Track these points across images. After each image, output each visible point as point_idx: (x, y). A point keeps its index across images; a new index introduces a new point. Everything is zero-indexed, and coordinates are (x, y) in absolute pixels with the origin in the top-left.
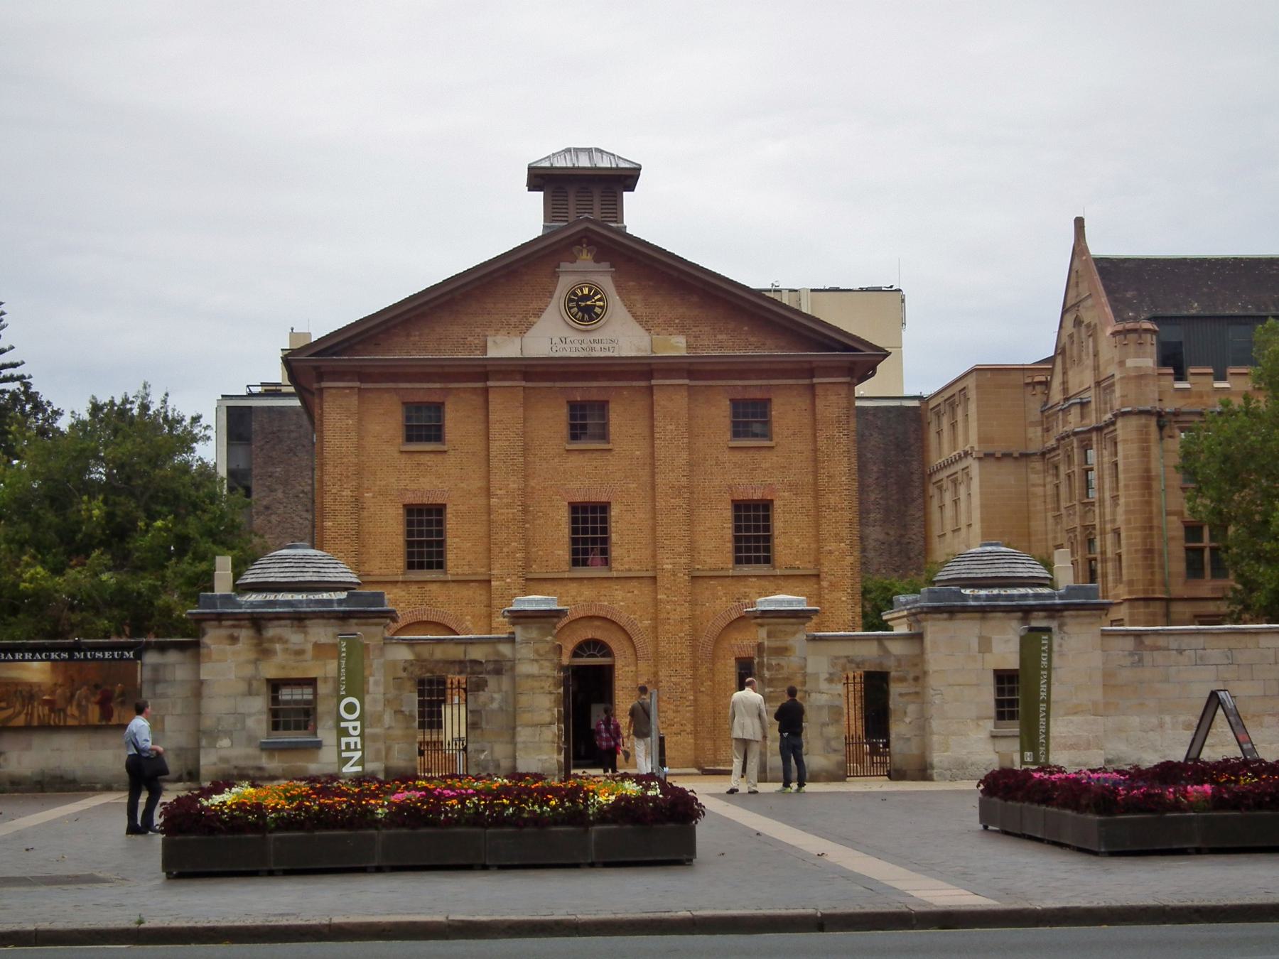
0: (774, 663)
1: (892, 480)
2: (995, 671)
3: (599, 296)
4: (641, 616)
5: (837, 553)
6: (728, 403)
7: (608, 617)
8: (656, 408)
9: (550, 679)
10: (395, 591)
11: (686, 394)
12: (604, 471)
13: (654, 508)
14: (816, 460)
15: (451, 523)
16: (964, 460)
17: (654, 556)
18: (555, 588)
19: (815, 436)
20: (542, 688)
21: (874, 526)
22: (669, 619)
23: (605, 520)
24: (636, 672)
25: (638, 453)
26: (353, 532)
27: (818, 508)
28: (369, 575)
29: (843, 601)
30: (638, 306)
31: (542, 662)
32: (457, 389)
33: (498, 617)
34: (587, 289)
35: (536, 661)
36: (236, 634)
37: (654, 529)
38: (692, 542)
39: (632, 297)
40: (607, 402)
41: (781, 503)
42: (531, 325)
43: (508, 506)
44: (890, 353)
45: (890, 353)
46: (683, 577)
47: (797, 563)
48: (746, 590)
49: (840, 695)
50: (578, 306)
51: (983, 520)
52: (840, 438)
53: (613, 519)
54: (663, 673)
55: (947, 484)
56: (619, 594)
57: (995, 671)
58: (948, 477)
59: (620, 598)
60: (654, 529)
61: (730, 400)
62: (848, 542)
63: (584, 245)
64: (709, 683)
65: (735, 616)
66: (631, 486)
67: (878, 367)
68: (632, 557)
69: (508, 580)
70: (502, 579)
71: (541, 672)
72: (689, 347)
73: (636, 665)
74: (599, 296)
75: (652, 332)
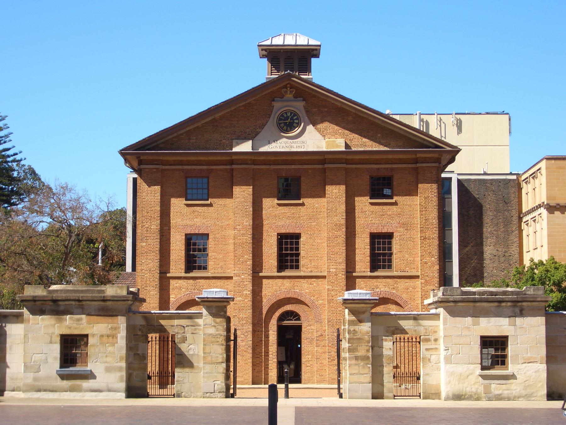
0: (352, 329)
1: (501, 220)
2: (482, 337)
3: (296, 117)
4: (317, 298)
6: (369, 177)
9: (222, 337)
11: (344, 172)
16: (539, 209)
20: (218, 342)
21: (490, 246)
22: (333, 300)
23: (297, 243)
31: (218, 327)
34: (289, 113)
35: (215, 326)
36: (44, 309)
40: (300, 177)
41: (399, 234)
42: (258, 133)
44: (461, 150)
48: (377, 284)
49: (390, 349)
50: (285, 124)
51: (549, 244)
55: (531, 222)
57: (482, 337)
58: (531, 219)
61: (370, 176)
62: (436, 257)
66: (313, 224)
67: (457, 157)
68: (313, 264)
70: (239, 276)
71: (217, 333)
72: (347, 146)
74: (296, 117)
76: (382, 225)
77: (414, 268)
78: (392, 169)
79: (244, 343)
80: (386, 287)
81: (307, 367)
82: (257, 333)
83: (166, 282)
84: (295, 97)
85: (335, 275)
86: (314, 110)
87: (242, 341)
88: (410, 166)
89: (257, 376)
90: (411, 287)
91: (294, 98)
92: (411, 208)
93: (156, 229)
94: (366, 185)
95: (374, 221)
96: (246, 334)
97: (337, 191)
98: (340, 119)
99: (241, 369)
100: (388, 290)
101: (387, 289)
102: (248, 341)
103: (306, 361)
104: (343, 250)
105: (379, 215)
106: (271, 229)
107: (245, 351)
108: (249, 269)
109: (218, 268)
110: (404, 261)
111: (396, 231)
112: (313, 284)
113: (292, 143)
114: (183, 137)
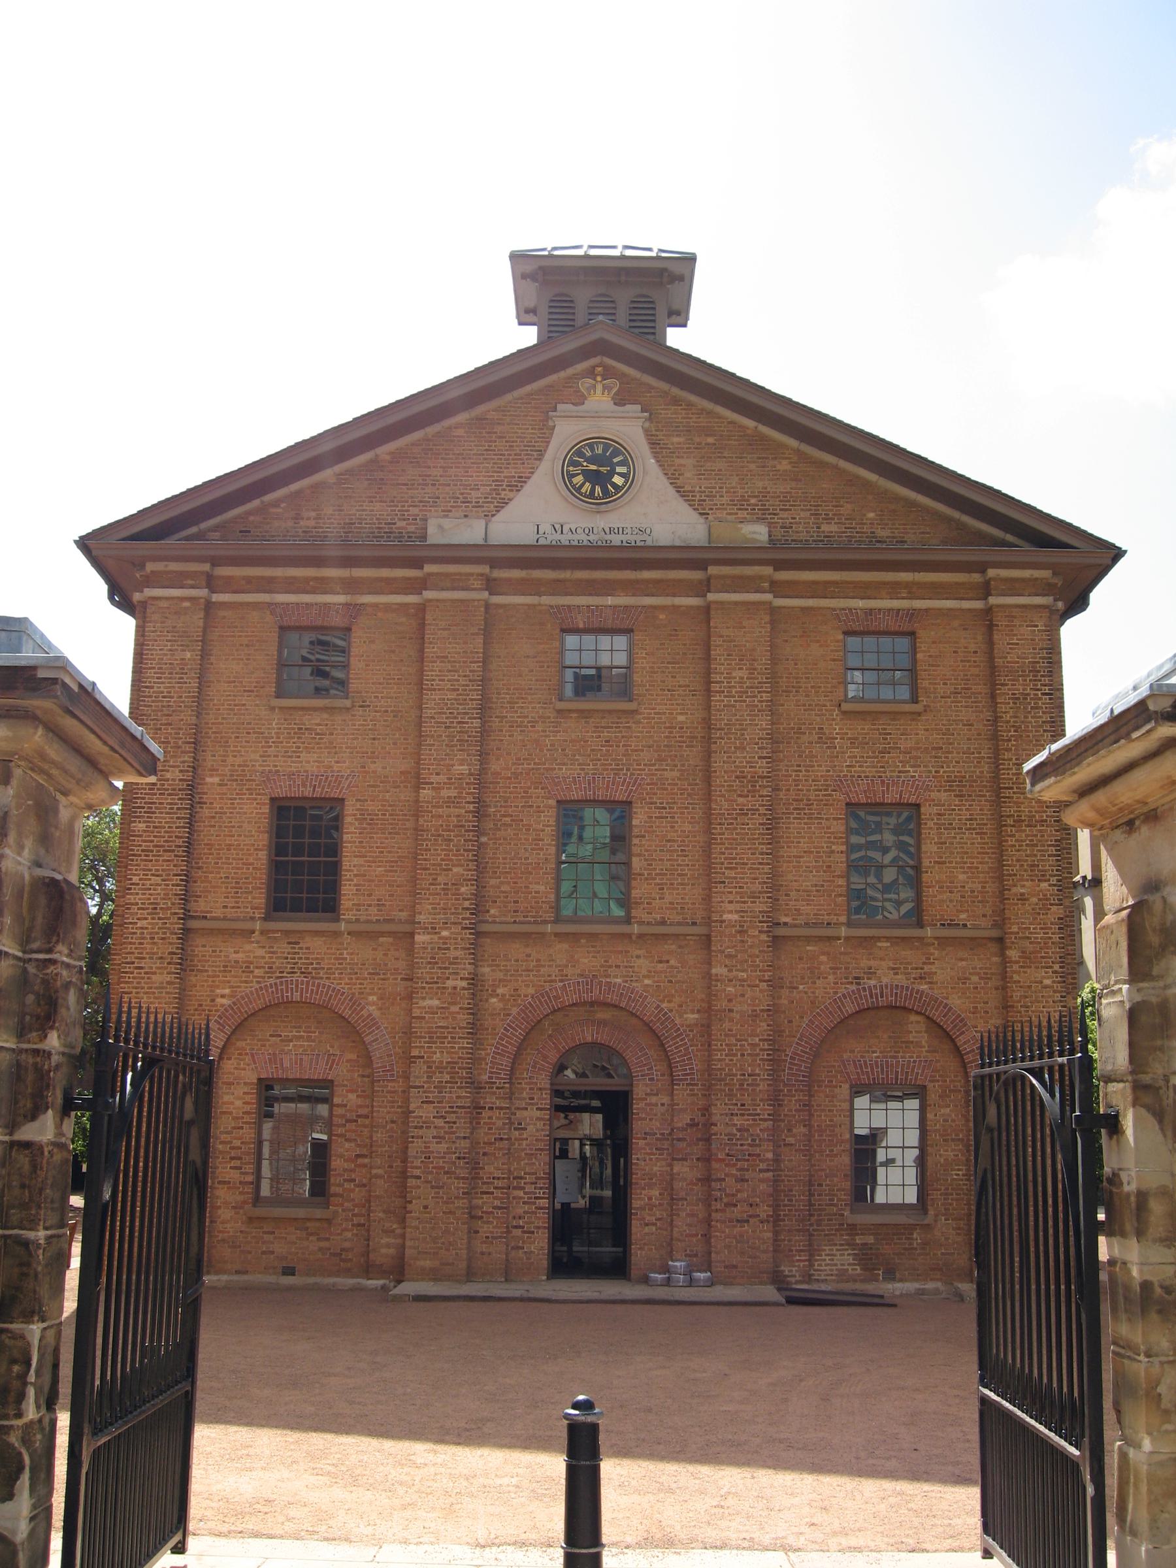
4: (681, 1006)
5: (1034, 900)
7: (623, 1005)
8: (715, 641)
10: (248, 947)
11: (767, 618)
12: (622, 749)
13: (708, 814)
14: (995, 737)
15: (351, 835)
17: (707, 899)
18: (528, 951)
19: (993, 696)
22: (731, 1011)
24: (672, 1105)
25: (681, 718)
26: (180, 842)
27: (999, 821)
28: (205, 918)
29: (1046, 987)
30: (688, 475)
32: (376, 605)
33: (424, 998)
37: (707, 852)
38: (775, 875)
39: (678, 461)
41: (935, 810)
42: (505, 503)
43: (450, 802)
45: (1125, 552)
46: (758, 937)
47: (963, 916)
48: (872, 963)
52: (1037, 698)
53: (635, 831)
54: (719, 1111)
56: (643, 964)
59: (644, 972)
60: (707, 852)
62: (1054, 880)
63: (599, 378)
64: (803, 1130)
65: (850, 1008)
68: (668, 898)
69: (445, 933)
70: (434, 930)
73: (672, 1094)
75: (710, 517)
76: (883, 782)
77: (984, 916)
78: (912, 614)
79: (443, 1147)
80: (896, 974)
81: (647, 1225)
82: (485, 1114)
83: (204, 946)
84: (620, 401)
85: (740, 932)
86: (675, 440)
87: (439, 1137)
88: (966, 605)
89: (482, 1253)
90: (978, 974)
91: (615, 404)
92: (970, 730)
93: (181, 780)
94: (834, 660)
95: (857, 769)
96: (451, 1117)
97: (744, 673)
98: (753, 466)
99: (433, 1228)
100: (905, 983)
101: (901, 980)
102: (458, 1138)
103: (642, 1208)
104: (762, 854)
105: (874, 752)
106: (536, 788)
107: (446, 1173)
108: (467, 909)
109: (370, 905)
110: (950, 892)
111: (926, 800)
112: (668, 962)
113: (607, 531)
114: (280, 510)
